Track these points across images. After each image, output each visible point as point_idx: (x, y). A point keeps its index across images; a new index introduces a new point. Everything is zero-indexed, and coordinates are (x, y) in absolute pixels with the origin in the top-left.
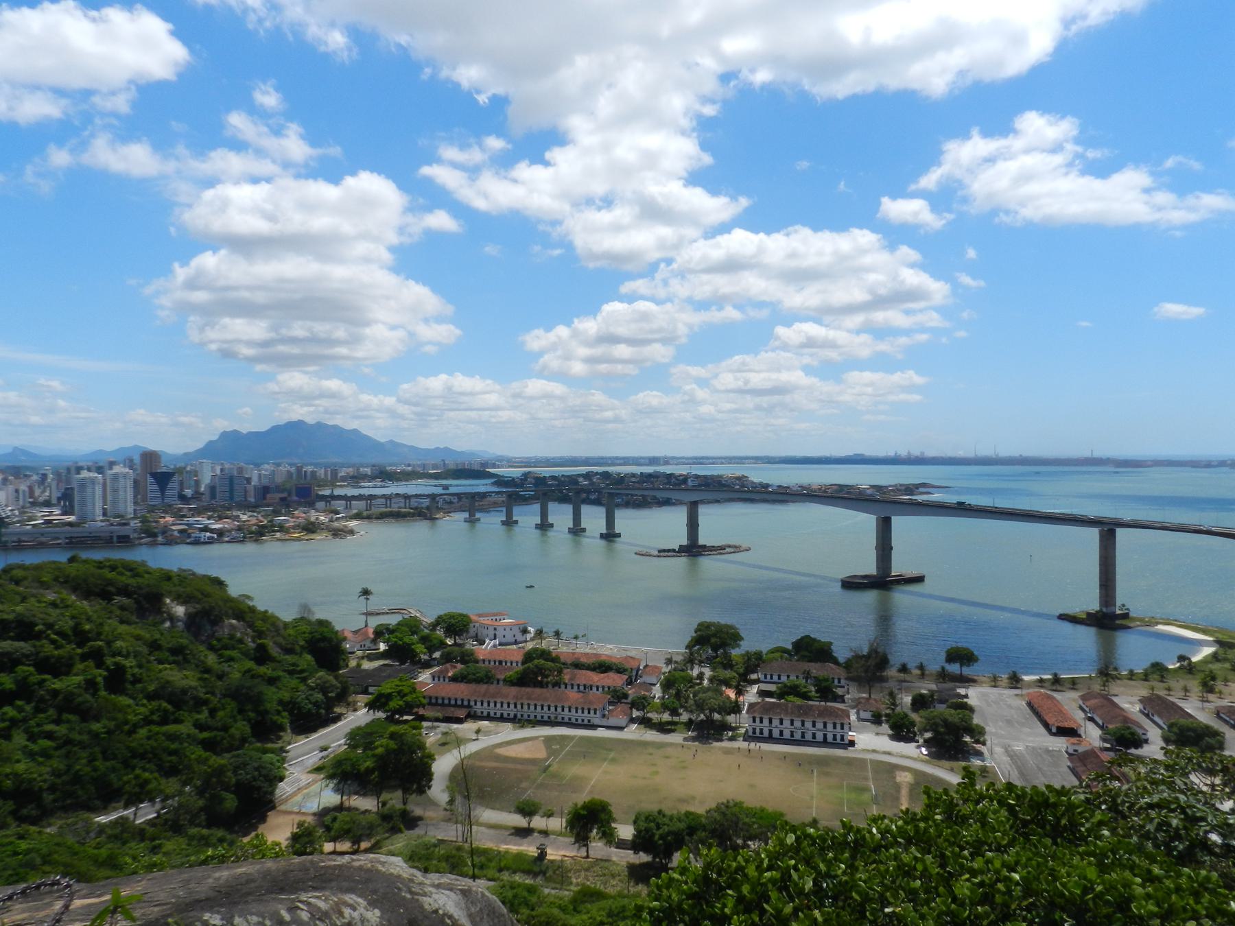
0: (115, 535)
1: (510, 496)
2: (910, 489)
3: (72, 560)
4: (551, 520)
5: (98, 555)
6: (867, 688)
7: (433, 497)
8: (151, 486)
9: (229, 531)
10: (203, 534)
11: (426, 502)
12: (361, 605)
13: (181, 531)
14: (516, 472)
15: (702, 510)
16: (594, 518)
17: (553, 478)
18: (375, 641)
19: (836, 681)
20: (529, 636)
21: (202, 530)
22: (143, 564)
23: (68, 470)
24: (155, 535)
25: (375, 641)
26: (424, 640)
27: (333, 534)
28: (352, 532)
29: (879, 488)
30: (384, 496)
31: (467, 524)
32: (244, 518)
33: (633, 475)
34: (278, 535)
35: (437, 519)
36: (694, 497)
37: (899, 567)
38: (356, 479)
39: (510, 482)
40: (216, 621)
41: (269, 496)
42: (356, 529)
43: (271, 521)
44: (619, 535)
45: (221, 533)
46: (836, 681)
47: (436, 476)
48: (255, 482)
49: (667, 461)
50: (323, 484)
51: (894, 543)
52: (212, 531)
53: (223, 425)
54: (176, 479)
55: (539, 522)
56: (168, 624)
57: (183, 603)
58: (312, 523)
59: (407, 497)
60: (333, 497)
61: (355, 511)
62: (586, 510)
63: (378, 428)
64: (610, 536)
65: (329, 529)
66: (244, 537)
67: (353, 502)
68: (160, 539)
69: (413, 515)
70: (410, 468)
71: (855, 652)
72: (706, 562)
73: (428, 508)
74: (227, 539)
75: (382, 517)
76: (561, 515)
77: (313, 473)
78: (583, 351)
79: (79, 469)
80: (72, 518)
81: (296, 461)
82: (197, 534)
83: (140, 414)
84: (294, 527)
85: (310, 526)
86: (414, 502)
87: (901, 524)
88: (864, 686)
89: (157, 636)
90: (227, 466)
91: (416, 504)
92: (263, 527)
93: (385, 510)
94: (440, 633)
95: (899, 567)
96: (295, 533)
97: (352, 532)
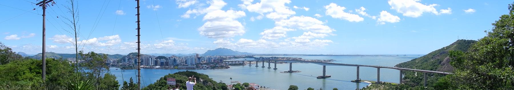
1: (257, 62)
2: (330, 61)
3: (187, 71)
4: (264, 66)
5: (190, 71)
7: (243, 61)
8: (197, 59)
14: (259, 57)
15: (292, 63)
16: (272, 65)
17: (265, 58)
18: (232, 87)
20: (259, 88)
21: (205, 67)
22: (196, 72)
23: (186, 57)
24: (198, 68)
25: (232, 87)
26: (241, 87)
28: (229, 68)
29: (324, 60)
30: (235, 61)
32: (211, 65)
33: (280, 57)
34: (217, 68)
36: (291, 62)
38: (230, 58)
39: (258, 59)
40: (207, 83)
41: (216, 61)
44: (277, 69)
45: (208, 67)
47: (244, 57)
48: (213, 59)
49: (287, 55)
50: (224, 59)
52: (206, 67)
53: (208, 49)
54: (201, 58)
56: (200, 82)
57: (202, 79)
59: (239, 61)
60: (226, 61)
63: (234, 49)
64: (275, 69)
65: (225, 67)
70: (239, 56)
72: (293, 74)
76: (266, 64)
77: (223, 57)
78: (271, 35)
79: (187, 57)
80: (187, 65)
81: (220, 55)
82: (204, 68)
83: (196, 48)
89: (199, 84)
90: (209, 56)
94: (244, 86)
97: (229, 68)
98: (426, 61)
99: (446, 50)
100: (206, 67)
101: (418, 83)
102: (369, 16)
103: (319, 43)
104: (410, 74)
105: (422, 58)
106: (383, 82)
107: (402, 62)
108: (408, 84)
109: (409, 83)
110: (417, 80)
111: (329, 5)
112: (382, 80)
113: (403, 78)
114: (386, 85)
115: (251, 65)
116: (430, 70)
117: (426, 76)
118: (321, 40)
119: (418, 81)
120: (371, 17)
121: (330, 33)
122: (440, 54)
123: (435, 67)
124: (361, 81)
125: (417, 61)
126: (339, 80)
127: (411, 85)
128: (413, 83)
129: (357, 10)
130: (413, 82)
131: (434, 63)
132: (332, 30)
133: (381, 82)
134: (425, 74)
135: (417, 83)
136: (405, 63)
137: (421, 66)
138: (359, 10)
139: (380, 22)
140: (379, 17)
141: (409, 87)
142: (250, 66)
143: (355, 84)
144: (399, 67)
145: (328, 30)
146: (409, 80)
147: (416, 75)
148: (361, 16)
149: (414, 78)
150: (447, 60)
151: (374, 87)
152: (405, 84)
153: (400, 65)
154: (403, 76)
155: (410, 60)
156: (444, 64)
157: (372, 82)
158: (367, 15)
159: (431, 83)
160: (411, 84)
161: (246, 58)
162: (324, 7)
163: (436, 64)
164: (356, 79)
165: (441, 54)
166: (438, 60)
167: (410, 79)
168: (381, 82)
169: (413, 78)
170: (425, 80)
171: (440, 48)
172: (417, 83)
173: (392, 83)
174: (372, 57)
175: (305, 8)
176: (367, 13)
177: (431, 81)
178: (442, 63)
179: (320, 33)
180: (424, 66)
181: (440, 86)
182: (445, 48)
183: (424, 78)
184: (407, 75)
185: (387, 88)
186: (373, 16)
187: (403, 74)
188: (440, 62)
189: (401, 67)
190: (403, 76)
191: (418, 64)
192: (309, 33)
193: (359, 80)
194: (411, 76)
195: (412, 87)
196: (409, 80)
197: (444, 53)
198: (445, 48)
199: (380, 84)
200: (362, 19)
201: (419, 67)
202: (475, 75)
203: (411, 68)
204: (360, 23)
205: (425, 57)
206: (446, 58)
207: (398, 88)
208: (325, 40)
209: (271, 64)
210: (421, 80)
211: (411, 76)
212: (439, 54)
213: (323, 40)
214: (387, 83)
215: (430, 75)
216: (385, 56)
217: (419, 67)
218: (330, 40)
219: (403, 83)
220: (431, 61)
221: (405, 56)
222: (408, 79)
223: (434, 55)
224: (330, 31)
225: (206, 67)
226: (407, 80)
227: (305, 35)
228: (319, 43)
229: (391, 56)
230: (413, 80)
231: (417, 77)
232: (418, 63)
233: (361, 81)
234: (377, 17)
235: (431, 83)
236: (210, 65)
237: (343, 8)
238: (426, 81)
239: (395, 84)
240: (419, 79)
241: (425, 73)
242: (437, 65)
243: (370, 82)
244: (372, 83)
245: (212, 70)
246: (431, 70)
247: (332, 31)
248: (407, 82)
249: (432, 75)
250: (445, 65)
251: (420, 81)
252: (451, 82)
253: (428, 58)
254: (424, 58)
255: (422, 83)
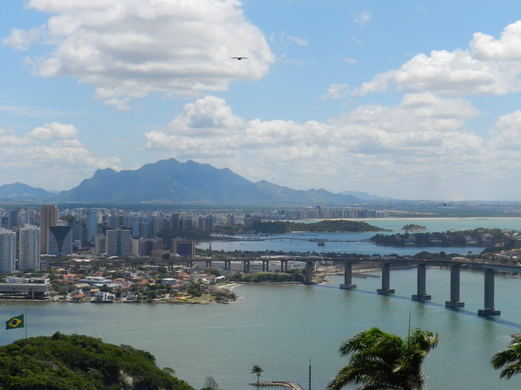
0: (33, 291)
4: (428, 292)
9: (125, 291)
10: (104, 294)
11: (302, 265)
12: (254, 378)
13: (85, 289)
27: (217, 299)
28: (233, 297)
31: (343, 291)
34: (167, 296)
35: (313, 283)
42: (237, 295)
43: (159, 282)
52: (109, 290)
55: (416, 294)
58: (197, 286)
61: (233, 273)
62: (465, 276)
66: (139, 298)
67: (232, 262)
68: (69, 297)
69: (289, 279)
73: (304, 272)
74: (125, 299)
75: (260, 280)
84: (182, 289)
85: (195, 290)
86: (292, 265)
91: (293, 268)
92: (153, 288)
93: (262, 273)
96: (182, 295)
97: (233, 297)
100: (109, 290)
115: (354, 281)
142: (347, 287)
161: (321, 236)
209: (465, 276)
225: (105, 289)
236: (128, 277)
245: (143, 308)
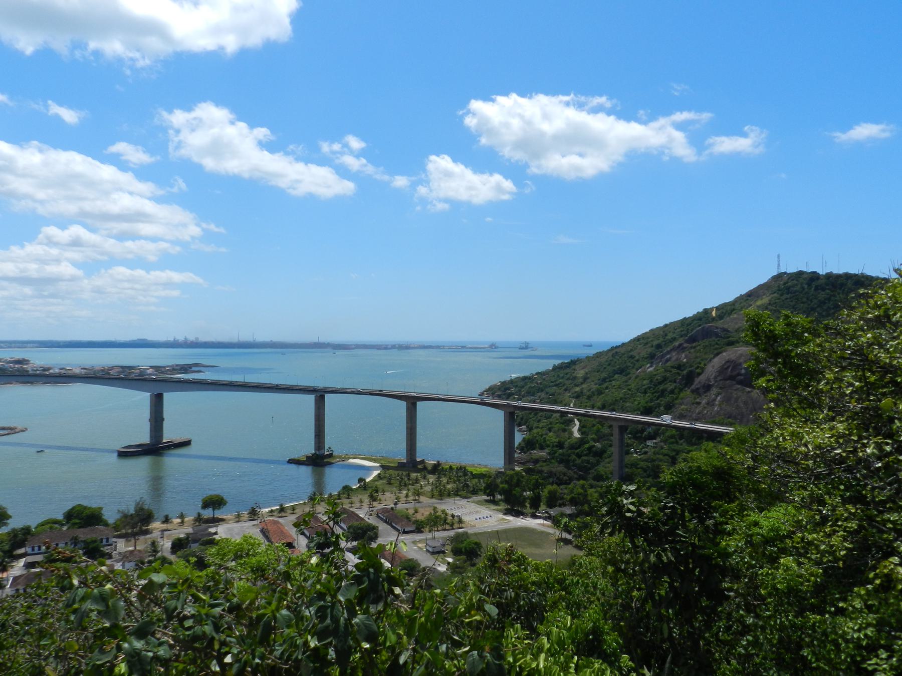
6: (133, 541)
19: (104, 541)
37: (169, 434)
46: (104, 541)
51: (165, 416)
71: (122, 512)
87: (171, 399)
88: (130, 541)
95: (169, 434)
98: (622, 371)
99: (720, 324)
101: (586, 470)
102: (378, 177)
103: (126, 285)
104: (550, 430)
105: (603, 360)
106: (431, 462)
107: (514, 376)
108: (541, 472)
109: (546, 469)
110: (579, 456)
111: (189, 109)
112: (427, 452)
113: (516, 444)
114: (445, 475)
116: (643, 414)
117: (621, 440)
118: (140, 273)
119: (584, 458)
120: (386, 178)
121: (193, 238)
122: (687, 341)
123: (663, 401)
124: (335, 457)
125: (580, 373)
126: (231, 459)
127: (551, 474)
128: (561, 468)
129: (325, 147)
130: (564, 461)
131: (660, 383)
132: (204, 225)
133: (423, 462)
134: (616, 431)
135: (580, 468)
136: (525, 378)
137: (600, 392)
138: (336, 147)
139: (424, 201)
140: (421, 182)
141: (544, 485)
143: (305, 472)
144: (499, 397)
145: (185, 225)
146: (543, 454)
147: (577, 435)
148: (343, 172)
149: (566, 445)
150: (722, 370)
151: (390, 483)
152: (529, 471)
153: (506, 389)
154: (519, 438)
155: (548, 365)
156: (708, 388)
157: (382, 462)
158: (370, 169)
159: (645, 471)
160: (554, 470)
162: (165, 114)
163: (670, 386)
164: (310, 450)
165: (692, 340)
166: (679, 367)
167: (547, 450)
168: (423, 462)
169: (560, 445)
170: (616, 456)
171: (689, 310)
172: (580, 468)
173: (473, 466)
174: (380, 352)
175: (55, 109)
176: (369, 161)
177: (642, 464)
178: (697, 380)
179: (134, 237)
180: (613, 394)
181: (698, 486)
182: (714, 314)
183: (614, 450)
184: (535, 431)
185: (449, 486)
186: (396, 177)
187: (516, 429)
188: (689, 379)
189: (507, 399)
190: (519, 438)
191: (584, 386)
192: (77, 230)
193: (324, 457)
194: (552, 437)
195: (559, 485)
196: (543, 454)
197: (707, 334)
198: (714, 314)
199: (418, 471)
200: (348, 187)
201: (589, 398)
202: (879, 446)
203: (555, 402)
204: (338, 201)
205: (616, 351)
206: (716, 360)
207: (497, 486)
208: (162, 270)
210: (600, 454)
211: (552, 437)
212: (681, 341)
213: (152, 273)
214: (451, 468)
215: (641, 433)
216: (438, 347)
217: (589, 398)
218: (191, 275)
219: (517, 468)
220: (644, 371)
221: (526, 348)
222: (542, 448)
223: (659, 346)
224: (194, 230)
226: (537, 453)
227: (51, 242)
228: (126, 285)
229: (463, 347)
230: (563, 454)
231: (582, 442)
232: (585, 379)
233: (335, 457)
234: (413, 178)
235: (645, 471)
237: (262, 132)
238: (621, 461)
239: (483, 470)
240: (590, 449)
241: (616, 425)
242: (672, 392)
243: (375, 461)
244: (383, 467)
246: (647, 412)
247: (203, 230)
248: (536, 461)
249: (651, 437)
250: (714, 391)
251: (592, 459)
252: (751, 470)
253: (632, 357)
254: (613, 356)
255: (601, 469)
